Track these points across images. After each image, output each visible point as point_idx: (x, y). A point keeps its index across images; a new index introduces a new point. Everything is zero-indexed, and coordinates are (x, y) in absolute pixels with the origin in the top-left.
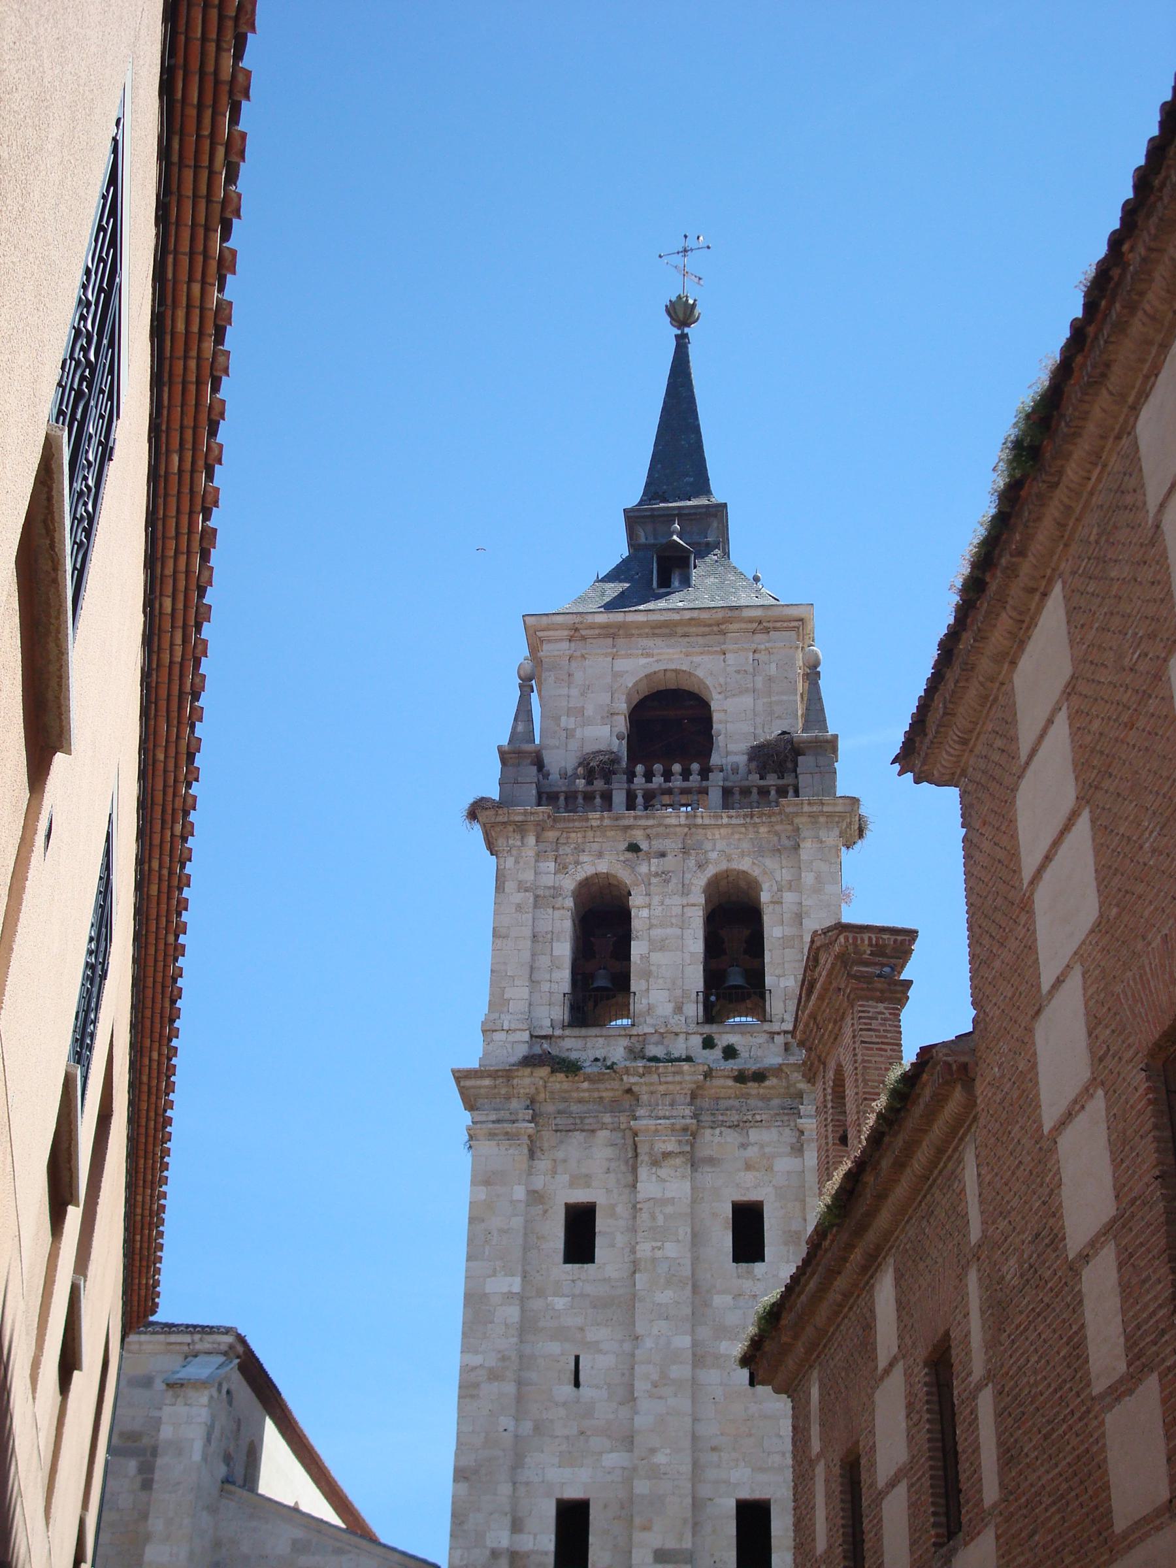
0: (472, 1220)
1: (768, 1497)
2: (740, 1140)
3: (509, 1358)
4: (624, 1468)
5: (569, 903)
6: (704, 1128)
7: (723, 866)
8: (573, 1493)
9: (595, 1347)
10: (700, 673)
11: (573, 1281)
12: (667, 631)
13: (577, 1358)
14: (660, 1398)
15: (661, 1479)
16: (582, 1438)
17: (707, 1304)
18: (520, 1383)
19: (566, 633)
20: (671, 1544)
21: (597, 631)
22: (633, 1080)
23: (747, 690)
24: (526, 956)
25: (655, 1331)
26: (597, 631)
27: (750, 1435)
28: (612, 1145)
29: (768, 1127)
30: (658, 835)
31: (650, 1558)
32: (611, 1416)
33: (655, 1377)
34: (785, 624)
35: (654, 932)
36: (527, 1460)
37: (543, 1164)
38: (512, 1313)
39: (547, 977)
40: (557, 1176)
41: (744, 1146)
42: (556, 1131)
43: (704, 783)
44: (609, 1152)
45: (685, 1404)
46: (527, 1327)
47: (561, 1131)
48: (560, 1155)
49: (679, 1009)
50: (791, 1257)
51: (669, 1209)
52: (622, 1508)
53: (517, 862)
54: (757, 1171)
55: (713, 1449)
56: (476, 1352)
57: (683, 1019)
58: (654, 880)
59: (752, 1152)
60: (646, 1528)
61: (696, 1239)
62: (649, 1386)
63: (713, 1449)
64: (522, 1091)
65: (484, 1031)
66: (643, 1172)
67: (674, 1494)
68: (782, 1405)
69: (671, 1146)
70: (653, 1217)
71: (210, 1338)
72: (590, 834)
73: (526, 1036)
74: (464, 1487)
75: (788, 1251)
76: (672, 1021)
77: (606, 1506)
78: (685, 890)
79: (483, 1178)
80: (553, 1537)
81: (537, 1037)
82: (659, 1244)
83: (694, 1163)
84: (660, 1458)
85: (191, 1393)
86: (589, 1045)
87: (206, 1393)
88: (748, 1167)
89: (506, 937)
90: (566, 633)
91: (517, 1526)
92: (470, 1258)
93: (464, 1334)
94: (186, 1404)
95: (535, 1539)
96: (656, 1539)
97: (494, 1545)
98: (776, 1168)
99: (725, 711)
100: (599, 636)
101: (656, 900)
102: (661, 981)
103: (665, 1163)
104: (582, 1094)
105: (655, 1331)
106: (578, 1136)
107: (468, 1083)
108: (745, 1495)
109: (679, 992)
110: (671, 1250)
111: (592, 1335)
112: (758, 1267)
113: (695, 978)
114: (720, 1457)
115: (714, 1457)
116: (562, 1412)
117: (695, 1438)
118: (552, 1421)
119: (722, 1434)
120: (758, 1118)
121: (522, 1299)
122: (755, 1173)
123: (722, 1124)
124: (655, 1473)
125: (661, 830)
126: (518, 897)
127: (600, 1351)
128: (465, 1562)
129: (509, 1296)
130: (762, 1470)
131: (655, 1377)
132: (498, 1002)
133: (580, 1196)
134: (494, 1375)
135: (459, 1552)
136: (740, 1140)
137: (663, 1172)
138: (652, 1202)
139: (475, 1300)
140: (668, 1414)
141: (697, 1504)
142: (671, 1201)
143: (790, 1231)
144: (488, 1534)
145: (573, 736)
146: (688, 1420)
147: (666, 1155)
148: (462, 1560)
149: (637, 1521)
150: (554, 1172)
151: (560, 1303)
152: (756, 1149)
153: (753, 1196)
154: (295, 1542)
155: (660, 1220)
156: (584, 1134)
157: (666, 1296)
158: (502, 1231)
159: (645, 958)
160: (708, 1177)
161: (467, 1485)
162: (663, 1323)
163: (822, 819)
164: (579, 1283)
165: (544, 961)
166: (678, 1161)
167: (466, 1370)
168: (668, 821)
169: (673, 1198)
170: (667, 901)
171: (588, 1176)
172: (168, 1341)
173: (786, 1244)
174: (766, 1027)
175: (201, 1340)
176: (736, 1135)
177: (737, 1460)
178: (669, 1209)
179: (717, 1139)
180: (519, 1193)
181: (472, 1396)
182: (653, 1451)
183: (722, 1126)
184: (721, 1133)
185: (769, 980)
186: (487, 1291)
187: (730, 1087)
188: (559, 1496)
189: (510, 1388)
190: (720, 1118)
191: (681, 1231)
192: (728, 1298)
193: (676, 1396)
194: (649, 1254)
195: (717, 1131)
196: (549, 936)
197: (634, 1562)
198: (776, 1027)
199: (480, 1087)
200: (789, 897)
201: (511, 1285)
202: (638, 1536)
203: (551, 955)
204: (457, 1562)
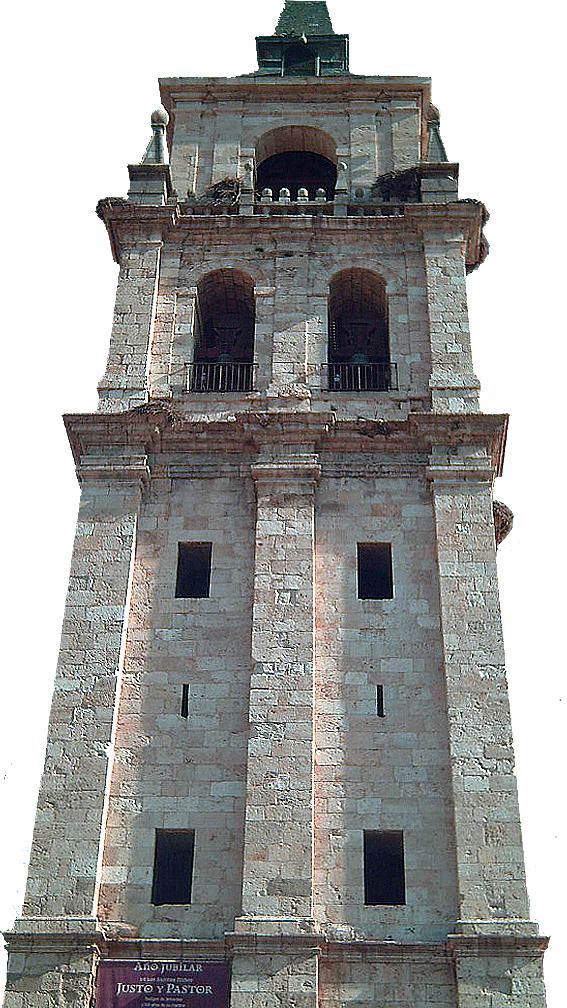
5: (194, 291)
7: (349, 265)
8: (172, 824)
9: (207, 677)
10: (326, 129)
12: (294, 96)
13: (186, 687)
19: (199, 95)
21: (228, 94)
26: (228, 94)
30: (283, 239)
41: (370, 494)
44: (226, 498)
48: (176, 499)
49: (301, 380)
52: (233, 838)
54: (384, 516)
59: (376, 500)
70: (274, 550)
78: (310, 283)
80: (151, 870)
90: (199, 95)
100: (231, 99)
104: (200, 445)
108: (374, 826)
111: (201, 666)
123: (348, 474)
125: (287, 233)
130: (396, 801)
133: (195, 536)
149: (249, 849)
150: (168, 515)
152: (383, 497)
153: (380, 539)
163: (446, 225)
170: (292, 292)
171: (206, 519)
174: (392, 394)
179: (342, 487)
182: (272, 776)
187: (354, 440)
198: (402, 395)
199: (92, 433)
200: (413, 291)
202: (249, 864)
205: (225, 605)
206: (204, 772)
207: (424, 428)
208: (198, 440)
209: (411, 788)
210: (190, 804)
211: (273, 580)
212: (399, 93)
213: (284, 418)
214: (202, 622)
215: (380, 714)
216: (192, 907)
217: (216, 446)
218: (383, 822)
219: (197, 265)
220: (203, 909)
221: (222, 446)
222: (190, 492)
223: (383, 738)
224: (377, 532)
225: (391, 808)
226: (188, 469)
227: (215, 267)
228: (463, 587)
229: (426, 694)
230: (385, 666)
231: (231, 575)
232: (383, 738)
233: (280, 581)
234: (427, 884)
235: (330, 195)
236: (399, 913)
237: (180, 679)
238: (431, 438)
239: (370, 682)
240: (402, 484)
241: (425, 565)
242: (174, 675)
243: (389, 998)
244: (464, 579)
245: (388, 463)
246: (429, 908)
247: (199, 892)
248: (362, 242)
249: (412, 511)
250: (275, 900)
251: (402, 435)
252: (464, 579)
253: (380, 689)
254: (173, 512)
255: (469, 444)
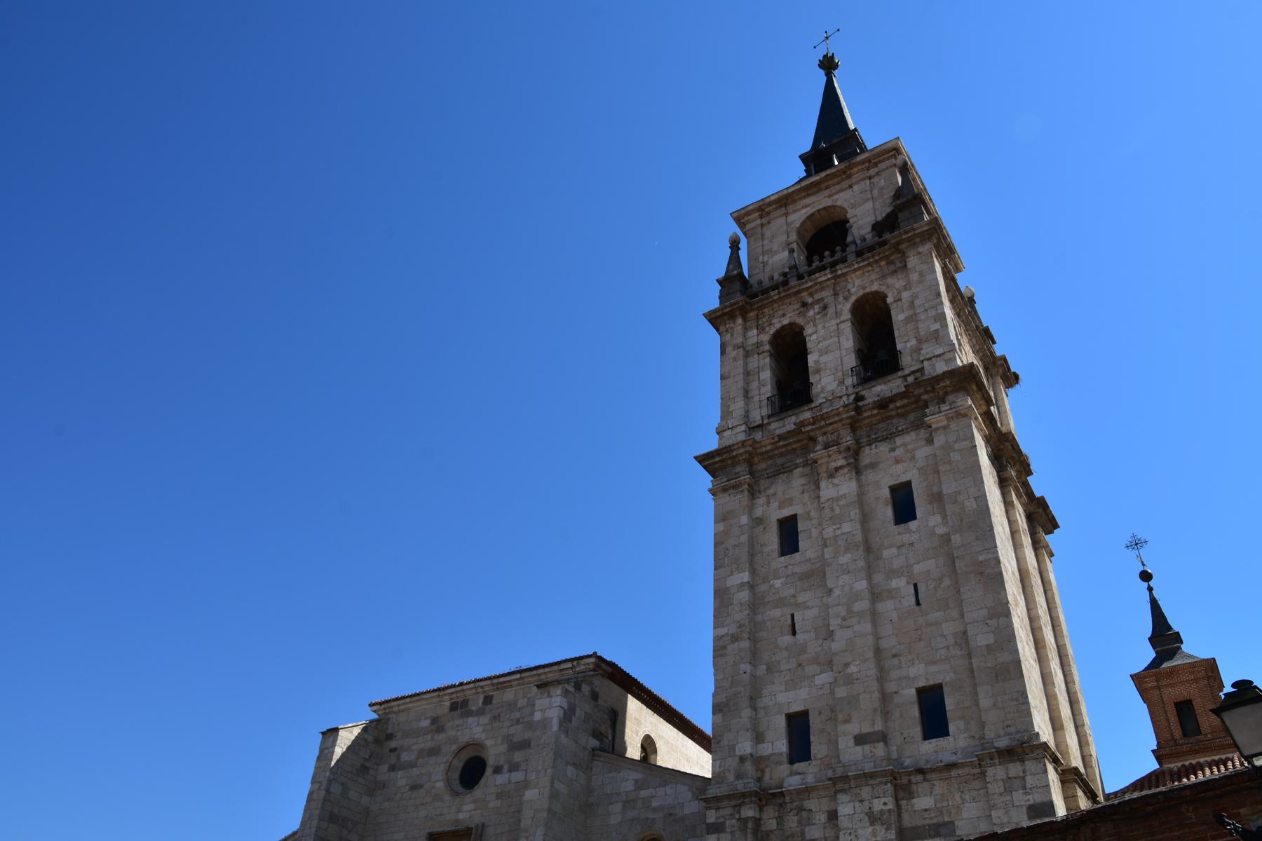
0: (716, 545)
1: (940, 681)
2: (890, 446)
3: (744, 625)
4: (830, 683)
6: (864, 446)
7: (861, 293)
8: (795, 708)
10: (839, 203)
11: (786, 567)
14: (849, 627)
15: (853, 683)
16: (799, 668)
17: (878, 558)
18: (754, 640)
19: (757, 214)
20: (866, 729)
21: (774, 206)
22: (808, 428)
23: (868, 200)
24: (741, 384)
25: (841, 583)
27: (920, 640)
28: (805, 476)
29: (908, 433)
30: (817, 291)
31: (852, 743)
32: (819, 649)
33: (843, 614)
34: (886, 156)
35: (820, 346)
36: (764, 691)
37: (761, 501)
38: (745, 595)
39: (757, 392)
40: (771, 504)
41: (893, 450)
42: (768, 478)
43: (844, 254)
44: (803, 481)
45: (867, 627)
46: (755, 605)
47: (771, 477)
48: (771, 491)
50: (935, 510)
51: (842, 502)
53: (732, 335)
54: (905, 462)
55: (895, 656)
56: (723, 626)
57: (844, 388)
58: (817, 317)
59: (899, 452)
60: (847, 721)
61: (865, 519)
62: (839, 621)
63: (895, 656)
64: (741, 458)
65: (718, 433)
66: (823, 484)
67: (864, 692)
68: (942, 613)
69: (841, 462)
70: (832, 510)
71: (582, 662)
72: (776, 305)
73: (743, 428)
74: (719, 717)
75: (933, 508)
76: (837, 391)
77: (820, 713)
79: (722, 517)
80: (785, 741)
81: (754, 428)
82: (838, 526)
83: (857, 470)
84: (853, 669)
85: (551, 689)
86: (786, 423)
87: (560, 687)
88: (898, 461)
89: (728, 377)
90: (757, 214)
91: (759, 738)
92: (716, 569)
93: (715, 616)
94: (548, 697)
95: (773, 745)
96: (854, 728)
97: (741, 754)
98: (917, 457)
99: (856, 216)
100: (777, 209)
101: (820, 327)
102: (828, 371)
103: (838, 474)
104: (780, 450)
105: (841, 583)
106: (783, 477)
107: (707, 463)
108: (922, 683)
109: (840, 374)
110: (846, 527)
111: (800, 599)
112: (913, 525)
113: (851, 361)
114: (900, 660)
115: (896, 661)
116: (785, 654)
117: (878, 651)
118: (779, 662)
119: (900, 644)
120: (900, 428)
121: (752, 586)
122: (904, 464)
123: (877, 440)
124: (850, 680)
126: (733, 354)
127: (808, 608)
128: (723, 768)
129: (743, 584)
130: (934, 663)
131: (843, 614)
132: (726, 413)
133: (786, 512)
134: (735, 638)
135: (718, 762)
136: (890, 446)
137: (835, 481)
138: (831, 501)
139: (721, 595)
140: (855, 636)
141: (885, 698)
142: (844, 496)
143: (933, 494)
144: (737, 746)
145: (767, 264)
146: (871, 638)
147: (837, 469)
148: (720, 767)
149: (840, 717)
151: (778, 583)
152: (901, 449)
153: (903, 479)
154: (636, 781)
155: (837, 510)
156: (786, 474)
157: (845, 559)
158: (734, 546)
159: (817, 362)
160: (869, 476)
161: (720, 715)
162: (846, 576)
163: (918, 240)
164: (790, 567)
165: (754, 385)
166: (846, 470)
167: (717, 639)
168: (820, 280)
169: (845, 495)
171: (791, 499)
172: (560, 668)
173: (931, 503)
174: (900, 373)
175: (578, 664)
176: (886, 444)
177: (913, 660)
178: (842, 502)
180: (744, 519)
181: (722, 655)
182: (847, 665)
183: (876, 442)
184: (876, 446)
185: (899, 347)
186: (728, 585)
188: (787, 712)
189: (745, 644)
190: (874, 437)
191: (852, 513)
192: (894, 551)
193: (859, 623)
194: (831, 534)
195: (874, 446)
196: (757, 370)
197: (840, 747)
198: (907, 372)
200: (905, 295)
201: (742, 578)
203: (759, 380)
204: (717, 770)
205: (811, 554)
206: (810, 670)
207: (917, 391)
208: (777, 448)
209: (944, 652)
210: (803, 693)
211: (834, 530)
212: (881, 158)
213: (825, 416)
214: (797, 569)
215: (918, 603)
216: (814, 763)
217: (790, 448)
218: (928, 679)
219: (767, 329)
220: (819, 762)
221: (795, 446)
222: (779, 487)
223: (921, 620)
224: (900, 473)
225: (933, 669)
226: (777, 468)
227: (778, 326)
228: (960, 498)
229: (947, 582)
230: (917, 569)
231: (811, 532)
232: (921, 620)
233: (838, 529)
234: (963, 718)
235: (844, 251)
236: (946, 742)
237: (788, 611)
238: (925, 397)
239: (908, 583)
240: (913, 435)
241: (935, 490)
242: (785, 609)
243: (945, 804)
244: (959, 493)
245: (901, 424)
246: (965, 735)
247: (816, 751)
248: (867, 274)
249: (923, 452)
250: (859, 748)
251: (905, 401)
252: (959, 493)
253: (915, 586)
254: (771, 501)
255: (952, 392)
